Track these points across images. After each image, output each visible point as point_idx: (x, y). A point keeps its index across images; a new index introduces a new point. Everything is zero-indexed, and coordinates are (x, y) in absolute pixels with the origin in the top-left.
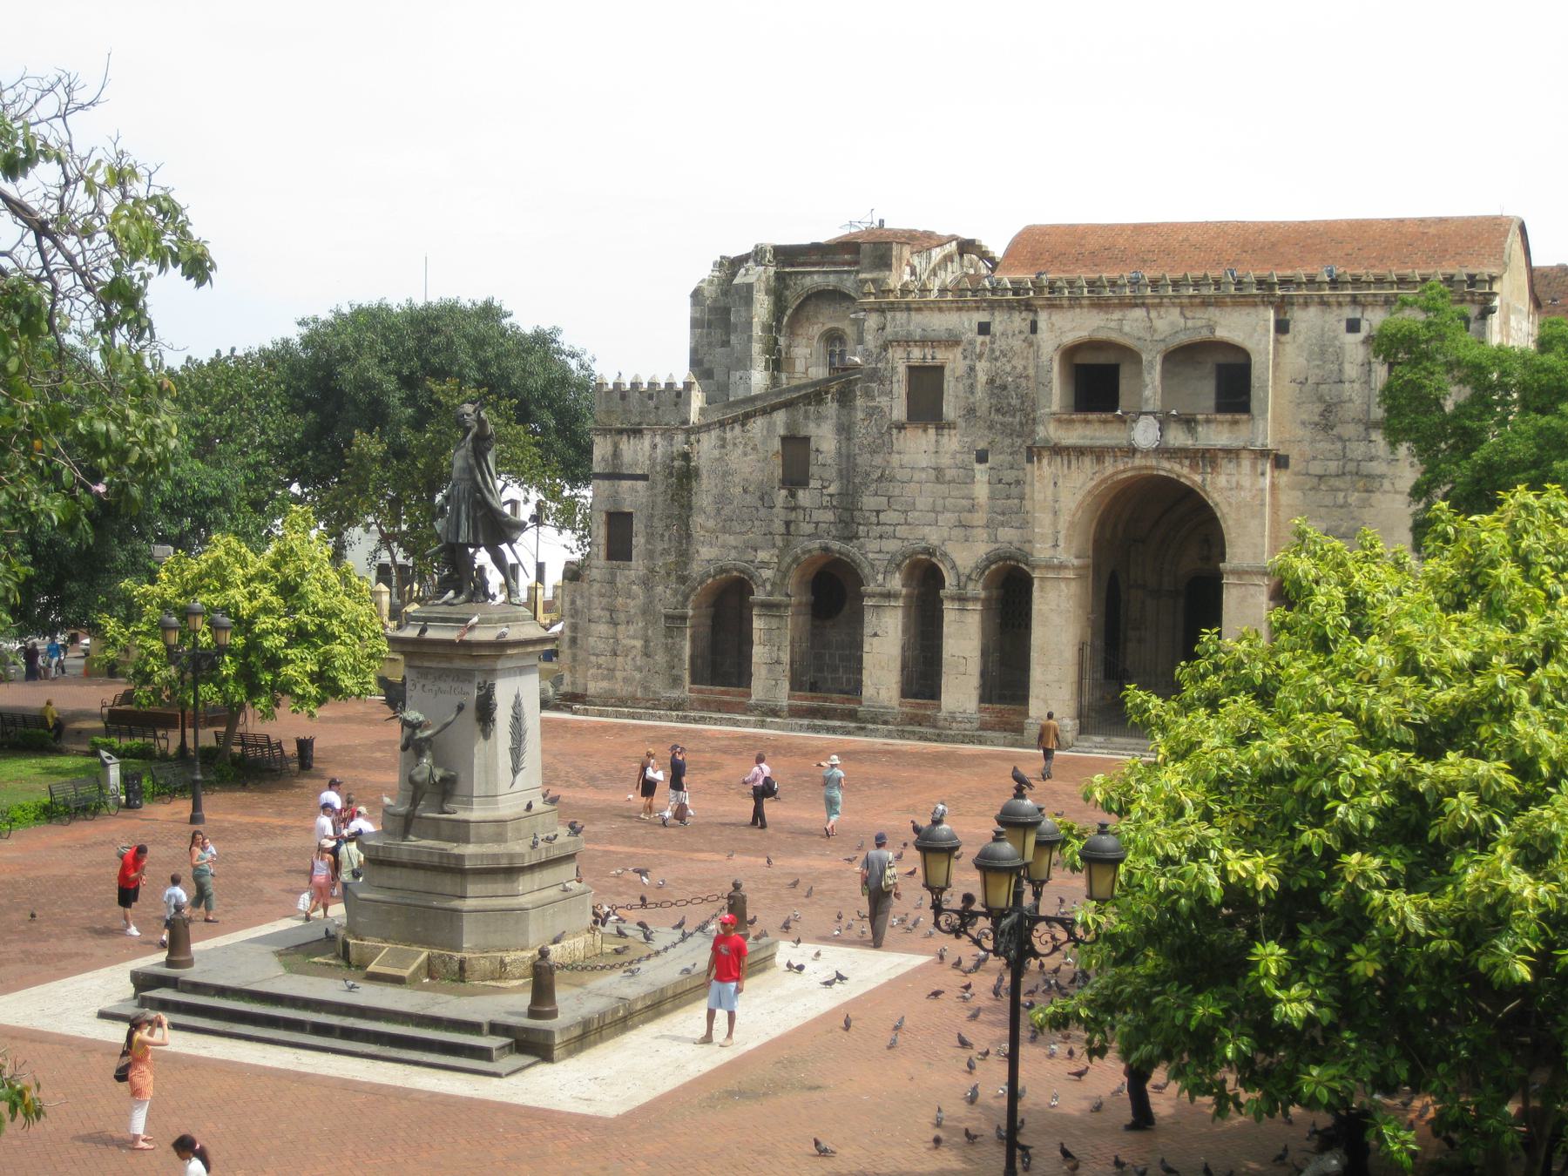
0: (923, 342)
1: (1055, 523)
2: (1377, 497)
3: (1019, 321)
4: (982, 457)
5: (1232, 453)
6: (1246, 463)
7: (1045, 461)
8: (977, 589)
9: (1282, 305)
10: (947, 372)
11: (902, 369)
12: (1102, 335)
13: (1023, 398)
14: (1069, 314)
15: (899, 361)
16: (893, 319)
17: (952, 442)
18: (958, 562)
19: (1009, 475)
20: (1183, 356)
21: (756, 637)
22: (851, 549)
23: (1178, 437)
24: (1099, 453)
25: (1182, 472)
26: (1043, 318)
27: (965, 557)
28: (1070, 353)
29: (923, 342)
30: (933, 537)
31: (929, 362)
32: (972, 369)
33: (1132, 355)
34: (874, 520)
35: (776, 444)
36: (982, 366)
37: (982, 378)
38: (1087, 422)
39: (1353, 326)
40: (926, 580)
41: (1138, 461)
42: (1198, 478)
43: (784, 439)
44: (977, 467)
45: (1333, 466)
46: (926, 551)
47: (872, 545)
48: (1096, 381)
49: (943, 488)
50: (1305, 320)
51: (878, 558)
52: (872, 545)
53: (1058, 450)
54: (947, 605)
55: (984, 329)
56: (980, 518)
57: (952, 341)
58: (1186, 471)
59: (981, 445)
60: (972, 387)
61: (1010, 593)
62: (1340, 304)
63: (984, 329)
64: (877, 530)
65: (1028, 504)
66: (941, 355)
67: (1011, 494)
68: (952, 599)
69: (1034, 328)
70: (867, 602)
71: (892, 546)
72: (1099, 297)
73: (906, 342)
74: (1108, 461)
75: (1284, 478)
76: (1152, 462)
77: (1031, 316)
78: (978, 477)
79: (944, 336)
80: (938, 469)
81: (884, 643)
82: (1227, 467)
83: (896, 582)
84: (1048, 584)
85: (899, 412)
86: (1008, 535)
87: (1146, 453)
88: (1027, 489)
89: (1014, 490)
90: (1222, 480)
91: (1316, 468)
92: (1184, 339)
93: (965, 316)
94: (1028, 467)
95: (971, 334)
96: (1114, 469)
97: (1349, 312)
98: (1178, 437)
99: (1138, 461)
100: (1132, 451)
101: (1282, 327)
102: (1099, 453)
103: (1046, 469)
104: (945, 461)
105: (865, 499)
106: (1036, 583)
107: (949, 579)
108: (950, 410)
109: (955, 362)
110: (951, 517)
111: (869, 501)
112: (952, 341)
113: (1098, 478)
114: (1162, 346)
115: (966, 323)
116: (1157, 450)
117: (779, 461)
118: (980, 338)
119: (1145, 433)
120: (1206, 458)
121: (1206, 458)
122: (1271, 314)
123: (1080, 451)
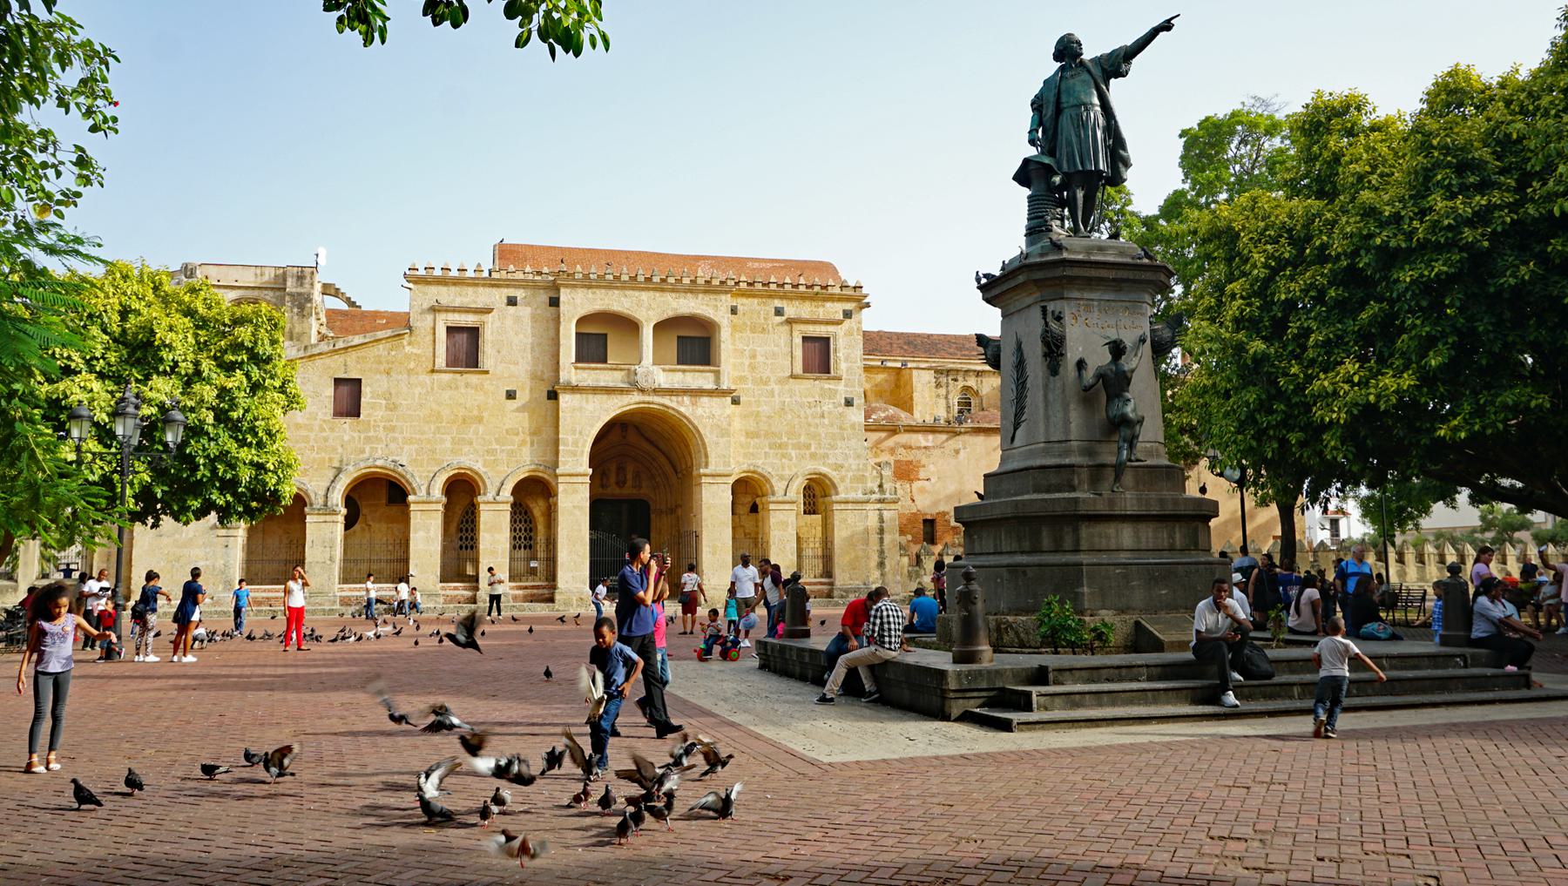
26: (565, 295)
33: (630, 326)
39: (779, 312)
61: (534, 496)
106: (561, 488)
115: (497, 297)
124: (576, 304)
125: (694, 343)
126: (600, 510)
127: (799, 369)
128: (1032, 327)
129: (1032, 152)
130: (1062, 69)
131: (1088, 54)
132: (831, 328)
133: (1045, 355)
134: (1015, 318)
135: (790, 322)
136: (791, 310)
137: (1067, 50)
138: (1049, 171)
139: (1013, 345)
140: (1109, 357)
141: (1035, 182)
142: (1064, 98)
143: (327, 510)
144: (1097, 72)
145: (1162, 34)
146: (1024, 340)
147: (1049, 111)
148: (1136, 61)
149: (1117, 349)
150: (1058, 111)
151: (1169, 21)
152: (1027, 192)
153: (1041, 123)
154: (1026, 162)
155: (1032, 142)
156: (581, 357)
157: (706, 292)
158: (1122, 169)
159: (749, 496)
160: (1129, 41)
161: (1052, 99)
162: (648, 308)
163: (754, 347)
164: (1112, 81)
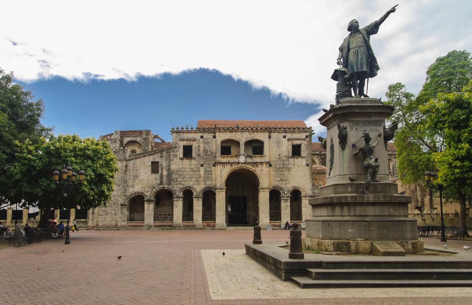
0: (187, 140)
1: (221, 179)
2: (290, 172)
3: (211, 135)
4: (202, 166)
5: (262, 163)
6: (264, 165)
7: (219, 166)
8: (201, 195)
9: (270, 132)
10: (193, 147)
11: (182, 146)
12: (231, 138)
13: (212, 152)
14: (223, 134)
15: (182, 144)
16: (180, 135)
17: (193, 162)
18: (197, 189)
19: (208, 170)
20: (248, 143)
21: (145, 209)
22: (170, 187)
23: (249, 160)
24: (231, 164)
25: (250, 167)
26: (217, 134)
27: (198, 188)
28: (223, 142)
29: (187, 140)
30: (190, 184)
31: (189, 144)
32: (199, 146)
33: (237, 143)
34: (176, 180)
35: (150, 164)
36: (202, 145)
37: (202, 148)
38: (228, 157)
39: (284, 137)
40: (188, 195)
41: (240, 165)
42: (254, 169)
43: (152, 162)
44: (201, 168)
45: (281, 166)
46: (189, 187)
47: (176, 186)
48: (227, 148)
49: (192, 173)
50: (273, 135)
51: (177, 189)
52: (175, 186)
53: (221, 163)
54: (194, 199)
55: (202, 137)
56: (202, 179)
57: (194, 140)
58: (251, 167)
59: (202, 163)
60: (199, 150)
61: (209, 196)
62: (282, 132)
63: (202, 137)
64: (177, 183)
65: (213, 176)
66: (192, 143)
67: (208, 173)
68: (196, 198)
69: (214, 137)
70: (174, 199)
71: (181, 186)
72: (231, 130)
73: (183, 140)
74: (233, 165)
75: (271, 168)
76: (243, 165)
77: (213, 135)
78: (201, 170)
79: (192, 138)
80: (192, 169)
81: (178, 208)
82: (260, 166)
83: (181, 195)
84: (220, 193)
85: (181, 156)
86: (208, 182)
87: (242, 164)
88: (213, 173)
89: (210, 173)
90: (259, 169)
91: (278, 167)
92: (249, 139)
93: (197, 134)
94: (213, 168)
95: (199, 138)
96: (235, 167)
97: (285, 134)
98: (249, 160)
99: (240, 165)
100: (239, 163)
101: (270, 137)
102: (231, 164)
103: (219, 167)
104: (193, 167)
105: (173, 176)
106: (217, 193)
107: (195, 194)
108: (194, 155)
109: (195, 145)
110: (195, 179)
111: (174, 176)
112: (194, 140)
113: (231, 169)
114: (245, 141)
116: (245, 163)
117: (151, 167)
118: (201, 139)
119: (242, 159)
120: (255, 164)
121: (255, 164)
122: (268, 134)
123: (227, 163)
124: (222, 137)
125: (256, 147)
126: (229, 200)
127: (291, 155)
128: (335, 131)
129: (338, 67)
130: (351, 34)
131: (361, 27)
132: (301, 142)
133: (340, 143)
134: (331, 130)
135: (289, 140)
136: (289, 136)
137: (353, 28)
138: (344, 73)
139: (330, 140)
140: (364, 142)
141: (339, 79)
142: (351, 45)
143: (149, 201)
144: (365, 33)
145: (391, 14)
146: (333, 138)
147: (345, 51)
148: (381, 27)
149: (367, 139)
150: (349, 50)
151: (394, 8)
152: (337, 82)
153: (342, 57)
154: (336, 71)
155: (338, 63)
156: (222, 153)
157: (261, 132)
158: (375, 70)
159: (275, 195)
160: (378, 18)
161: (346, 46)
162: (243, 137)
163: (276, 147)
164: (371, 36)
